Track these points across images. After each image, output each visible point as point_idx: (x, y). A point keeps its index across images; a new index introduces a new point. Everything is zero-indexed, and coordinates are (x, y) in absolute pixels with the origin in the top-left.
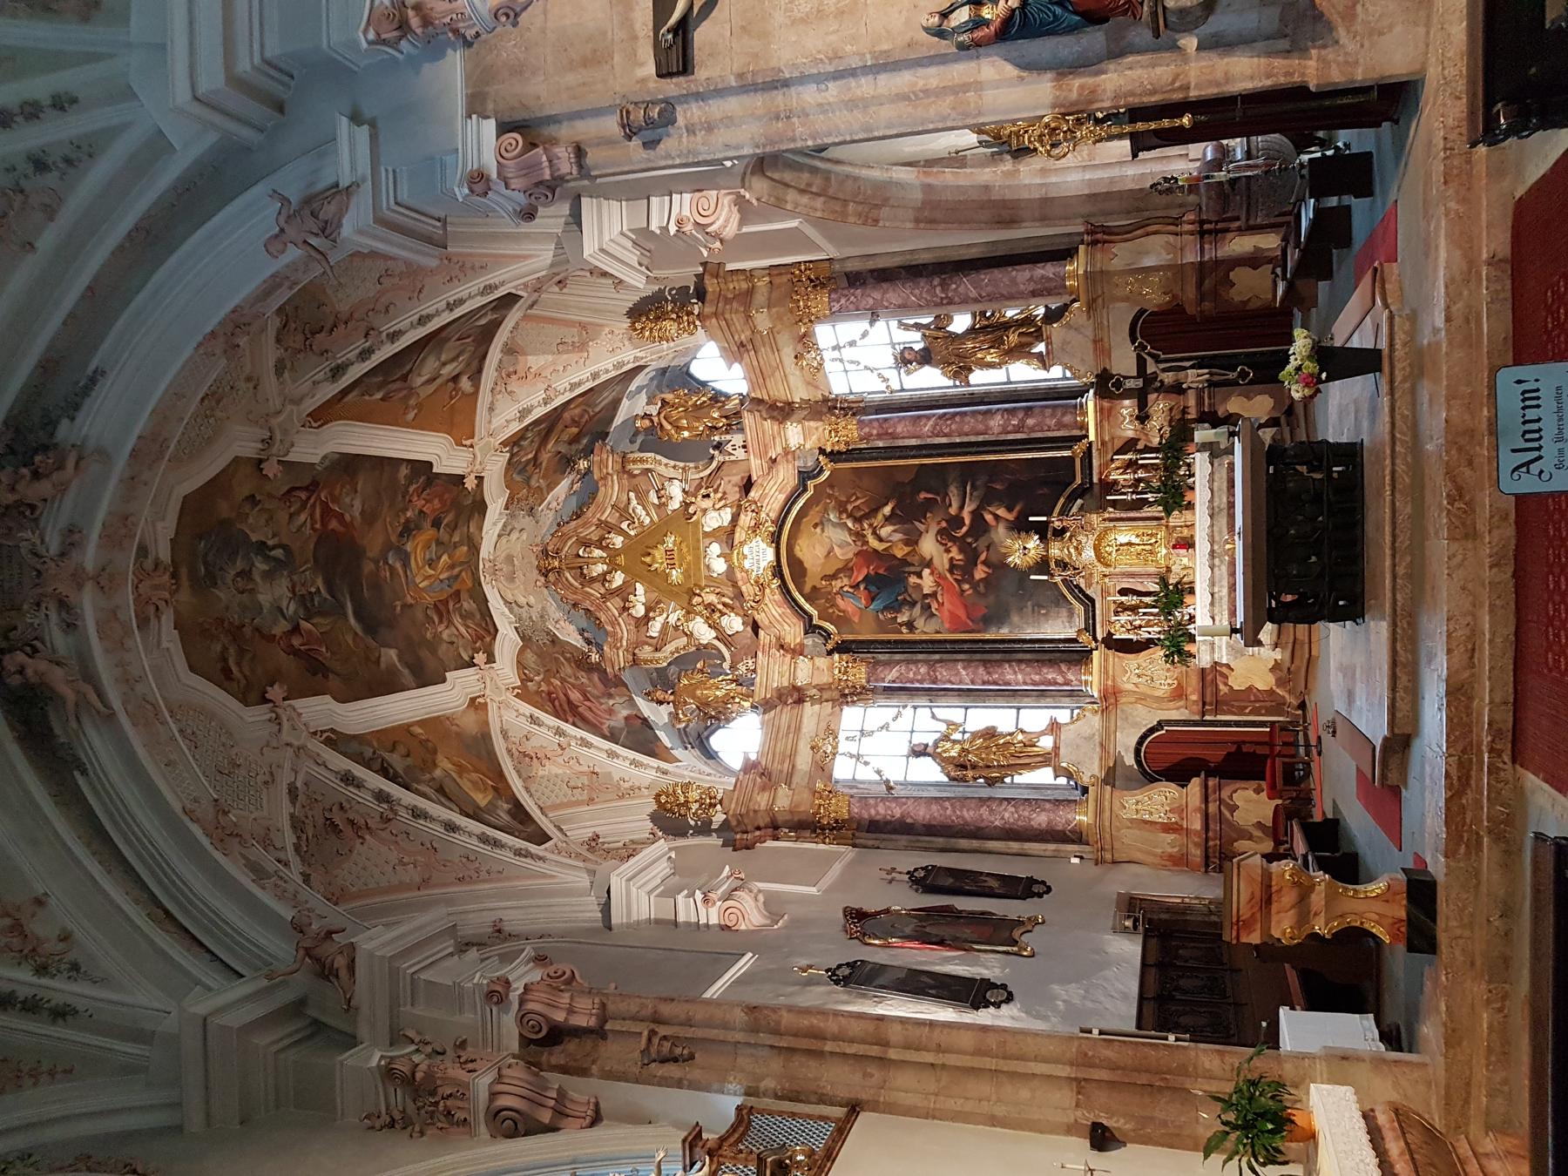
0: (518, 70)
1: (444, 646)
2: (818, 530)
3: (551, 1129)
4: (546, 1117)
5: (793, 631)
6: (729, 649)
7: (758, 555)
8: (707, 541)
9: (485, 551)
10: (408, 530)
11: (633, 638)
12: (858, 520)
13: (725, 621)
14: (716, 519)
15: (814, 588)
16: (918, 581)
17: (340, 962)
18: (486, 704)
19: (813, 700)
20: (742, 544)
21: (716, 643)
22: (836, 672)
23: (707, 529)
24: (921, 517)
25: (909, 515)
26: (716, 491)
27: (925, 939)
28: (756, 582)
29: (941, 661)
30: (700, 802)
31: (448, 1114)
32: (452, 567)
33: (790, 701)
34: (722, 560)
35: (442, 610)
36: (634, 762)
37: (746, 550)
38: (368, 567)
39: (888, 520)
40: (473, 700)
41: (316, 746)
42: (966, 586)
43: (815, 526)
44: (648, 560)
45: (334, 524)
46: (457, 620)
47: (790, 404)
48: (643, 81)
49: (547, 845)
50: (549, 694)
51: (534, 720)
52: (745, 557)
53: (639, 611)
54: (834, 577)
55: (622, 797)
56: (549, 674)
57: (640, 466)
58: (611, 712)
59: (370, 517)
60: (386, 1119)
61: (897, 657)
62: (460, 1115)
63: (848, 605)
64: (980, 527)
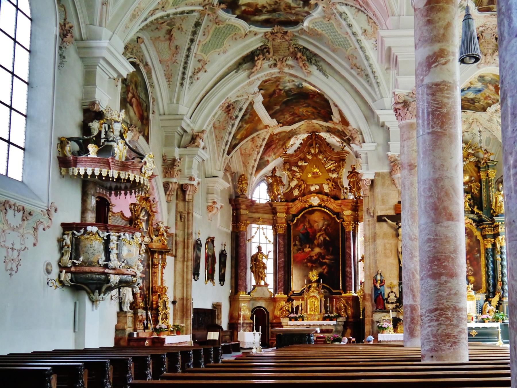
0: (383, 184)
1: (282, 117)
2: (322, 218)
3: (166, 193)
4: (168, 193)
5: (293, 211)
6: (288, 192)
7: (315, 201)
8: (320, 185)
9: (315, 121)
10: (314, 107)
11: (292, 162)
12: (325, 230)
13: (297, 190)
14: (326, 188)
15: (306, 217)
16: (307, 247)
17: (196, 144)
18: (267, 128)
19: (273, 217)
20: (318, 197)
21: (290, 188)
22: (281, 225)
23: (323, 185)
24: (325, 248)
25: (325, 245)
26: (334, 188)
27: (207, 258)
28: (307, 201)
29: (285, 254)
30: (243, 188)
31: (167, 173)
32: (307, 115)
33: (273, 210)
34: (314, 189)
35: (294, 114)
36: (253, 167)
37: (316, 198)
38: (303, 101)
39: (325, 239)
40: (268, 126)
41: (248, 102)
42: (306, 261)
43: (324, 218)
44: (315, 167)
45: (311, 96)
46: (291, 118)
47: (357, 211)
48: (377, 212)
49: (227, 156)
50: (273, 141)
51: (264, 139)
52: (314, 197)
53: (300, 164)
54: (309, 223)
55: (243, 163)
56: (279, 140)
57: (341, 165)
58: (269, 156)
59: (316, 102)
60: (165, 158)
61: (286, 241)
62: (167, 175)
63: (301, 228)
64: (322, 264)
